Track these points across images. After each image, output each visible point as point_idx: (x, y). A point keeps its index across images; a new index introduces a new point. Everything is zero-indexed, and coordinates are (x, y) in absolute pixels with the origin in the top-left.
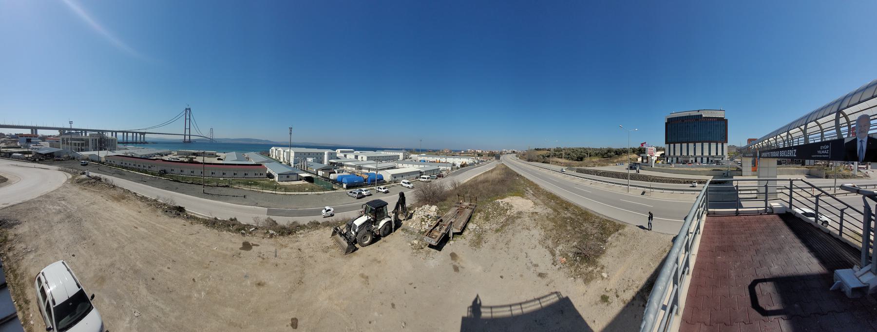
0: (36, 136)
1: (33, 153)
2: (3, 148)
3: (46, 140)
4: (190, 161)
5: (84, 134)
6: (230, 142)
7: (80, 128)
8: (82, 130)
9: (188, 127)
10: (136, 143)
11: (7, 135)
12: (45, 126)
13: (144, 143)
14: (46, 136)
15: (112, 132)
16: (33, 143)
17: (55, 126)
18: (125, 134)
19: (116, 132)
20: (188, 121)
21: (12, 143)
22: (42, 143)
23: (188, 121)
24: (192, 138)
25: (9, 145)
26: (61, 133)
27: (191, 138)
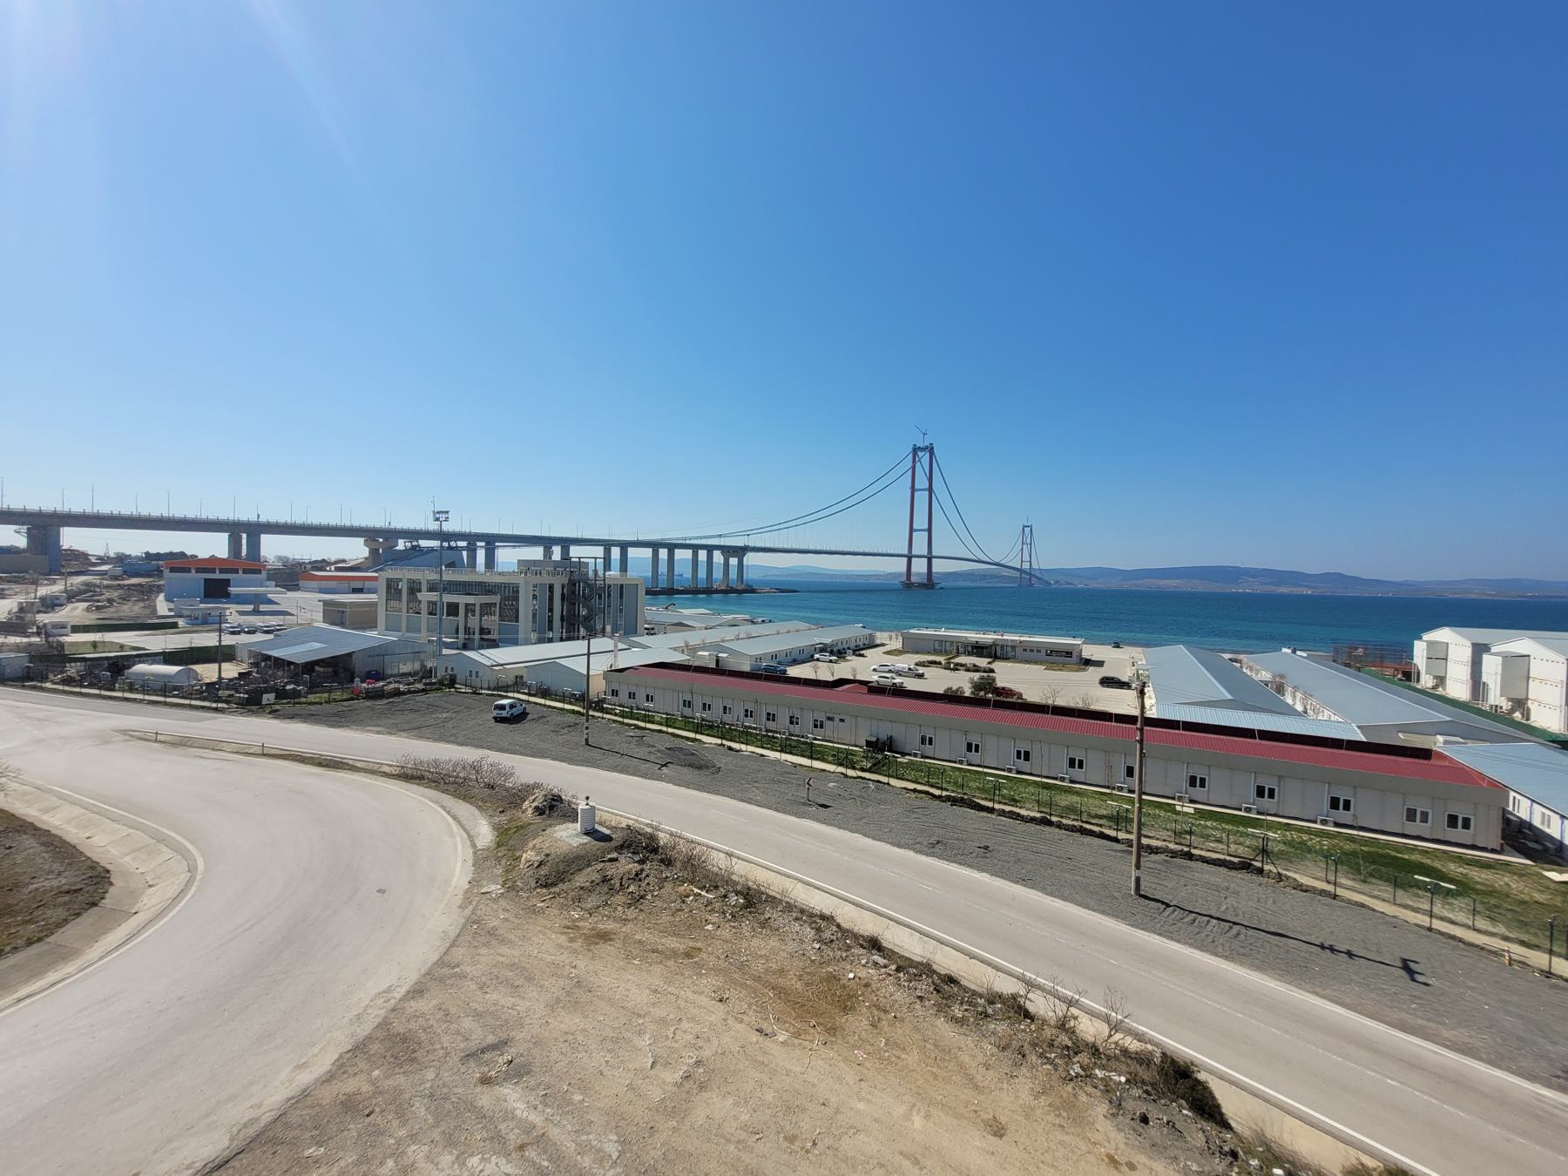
0: (254, 565)
1: (242, 654)
2: (76, 629)
3: (302, 583)
4: (977, 687)
5: (481, 555)
7: (466, 529)
8: (472, 538)
9: (921, 522)
10: (709, 591)
11: (103, 560)
12: (299, 519)
13: (739, 591)
14: (301, 564)
15: (607, 545)
16: (240, 599)
17: (346, 522)
18: (663, 553)
19: (624, 546)
20: (921, 498)
21: (124, 599)
22: (287, 599)
23: (921, 498)
24: (939, 567)
25: (110, 612)
26: (374, 552)
27: (934, 570)
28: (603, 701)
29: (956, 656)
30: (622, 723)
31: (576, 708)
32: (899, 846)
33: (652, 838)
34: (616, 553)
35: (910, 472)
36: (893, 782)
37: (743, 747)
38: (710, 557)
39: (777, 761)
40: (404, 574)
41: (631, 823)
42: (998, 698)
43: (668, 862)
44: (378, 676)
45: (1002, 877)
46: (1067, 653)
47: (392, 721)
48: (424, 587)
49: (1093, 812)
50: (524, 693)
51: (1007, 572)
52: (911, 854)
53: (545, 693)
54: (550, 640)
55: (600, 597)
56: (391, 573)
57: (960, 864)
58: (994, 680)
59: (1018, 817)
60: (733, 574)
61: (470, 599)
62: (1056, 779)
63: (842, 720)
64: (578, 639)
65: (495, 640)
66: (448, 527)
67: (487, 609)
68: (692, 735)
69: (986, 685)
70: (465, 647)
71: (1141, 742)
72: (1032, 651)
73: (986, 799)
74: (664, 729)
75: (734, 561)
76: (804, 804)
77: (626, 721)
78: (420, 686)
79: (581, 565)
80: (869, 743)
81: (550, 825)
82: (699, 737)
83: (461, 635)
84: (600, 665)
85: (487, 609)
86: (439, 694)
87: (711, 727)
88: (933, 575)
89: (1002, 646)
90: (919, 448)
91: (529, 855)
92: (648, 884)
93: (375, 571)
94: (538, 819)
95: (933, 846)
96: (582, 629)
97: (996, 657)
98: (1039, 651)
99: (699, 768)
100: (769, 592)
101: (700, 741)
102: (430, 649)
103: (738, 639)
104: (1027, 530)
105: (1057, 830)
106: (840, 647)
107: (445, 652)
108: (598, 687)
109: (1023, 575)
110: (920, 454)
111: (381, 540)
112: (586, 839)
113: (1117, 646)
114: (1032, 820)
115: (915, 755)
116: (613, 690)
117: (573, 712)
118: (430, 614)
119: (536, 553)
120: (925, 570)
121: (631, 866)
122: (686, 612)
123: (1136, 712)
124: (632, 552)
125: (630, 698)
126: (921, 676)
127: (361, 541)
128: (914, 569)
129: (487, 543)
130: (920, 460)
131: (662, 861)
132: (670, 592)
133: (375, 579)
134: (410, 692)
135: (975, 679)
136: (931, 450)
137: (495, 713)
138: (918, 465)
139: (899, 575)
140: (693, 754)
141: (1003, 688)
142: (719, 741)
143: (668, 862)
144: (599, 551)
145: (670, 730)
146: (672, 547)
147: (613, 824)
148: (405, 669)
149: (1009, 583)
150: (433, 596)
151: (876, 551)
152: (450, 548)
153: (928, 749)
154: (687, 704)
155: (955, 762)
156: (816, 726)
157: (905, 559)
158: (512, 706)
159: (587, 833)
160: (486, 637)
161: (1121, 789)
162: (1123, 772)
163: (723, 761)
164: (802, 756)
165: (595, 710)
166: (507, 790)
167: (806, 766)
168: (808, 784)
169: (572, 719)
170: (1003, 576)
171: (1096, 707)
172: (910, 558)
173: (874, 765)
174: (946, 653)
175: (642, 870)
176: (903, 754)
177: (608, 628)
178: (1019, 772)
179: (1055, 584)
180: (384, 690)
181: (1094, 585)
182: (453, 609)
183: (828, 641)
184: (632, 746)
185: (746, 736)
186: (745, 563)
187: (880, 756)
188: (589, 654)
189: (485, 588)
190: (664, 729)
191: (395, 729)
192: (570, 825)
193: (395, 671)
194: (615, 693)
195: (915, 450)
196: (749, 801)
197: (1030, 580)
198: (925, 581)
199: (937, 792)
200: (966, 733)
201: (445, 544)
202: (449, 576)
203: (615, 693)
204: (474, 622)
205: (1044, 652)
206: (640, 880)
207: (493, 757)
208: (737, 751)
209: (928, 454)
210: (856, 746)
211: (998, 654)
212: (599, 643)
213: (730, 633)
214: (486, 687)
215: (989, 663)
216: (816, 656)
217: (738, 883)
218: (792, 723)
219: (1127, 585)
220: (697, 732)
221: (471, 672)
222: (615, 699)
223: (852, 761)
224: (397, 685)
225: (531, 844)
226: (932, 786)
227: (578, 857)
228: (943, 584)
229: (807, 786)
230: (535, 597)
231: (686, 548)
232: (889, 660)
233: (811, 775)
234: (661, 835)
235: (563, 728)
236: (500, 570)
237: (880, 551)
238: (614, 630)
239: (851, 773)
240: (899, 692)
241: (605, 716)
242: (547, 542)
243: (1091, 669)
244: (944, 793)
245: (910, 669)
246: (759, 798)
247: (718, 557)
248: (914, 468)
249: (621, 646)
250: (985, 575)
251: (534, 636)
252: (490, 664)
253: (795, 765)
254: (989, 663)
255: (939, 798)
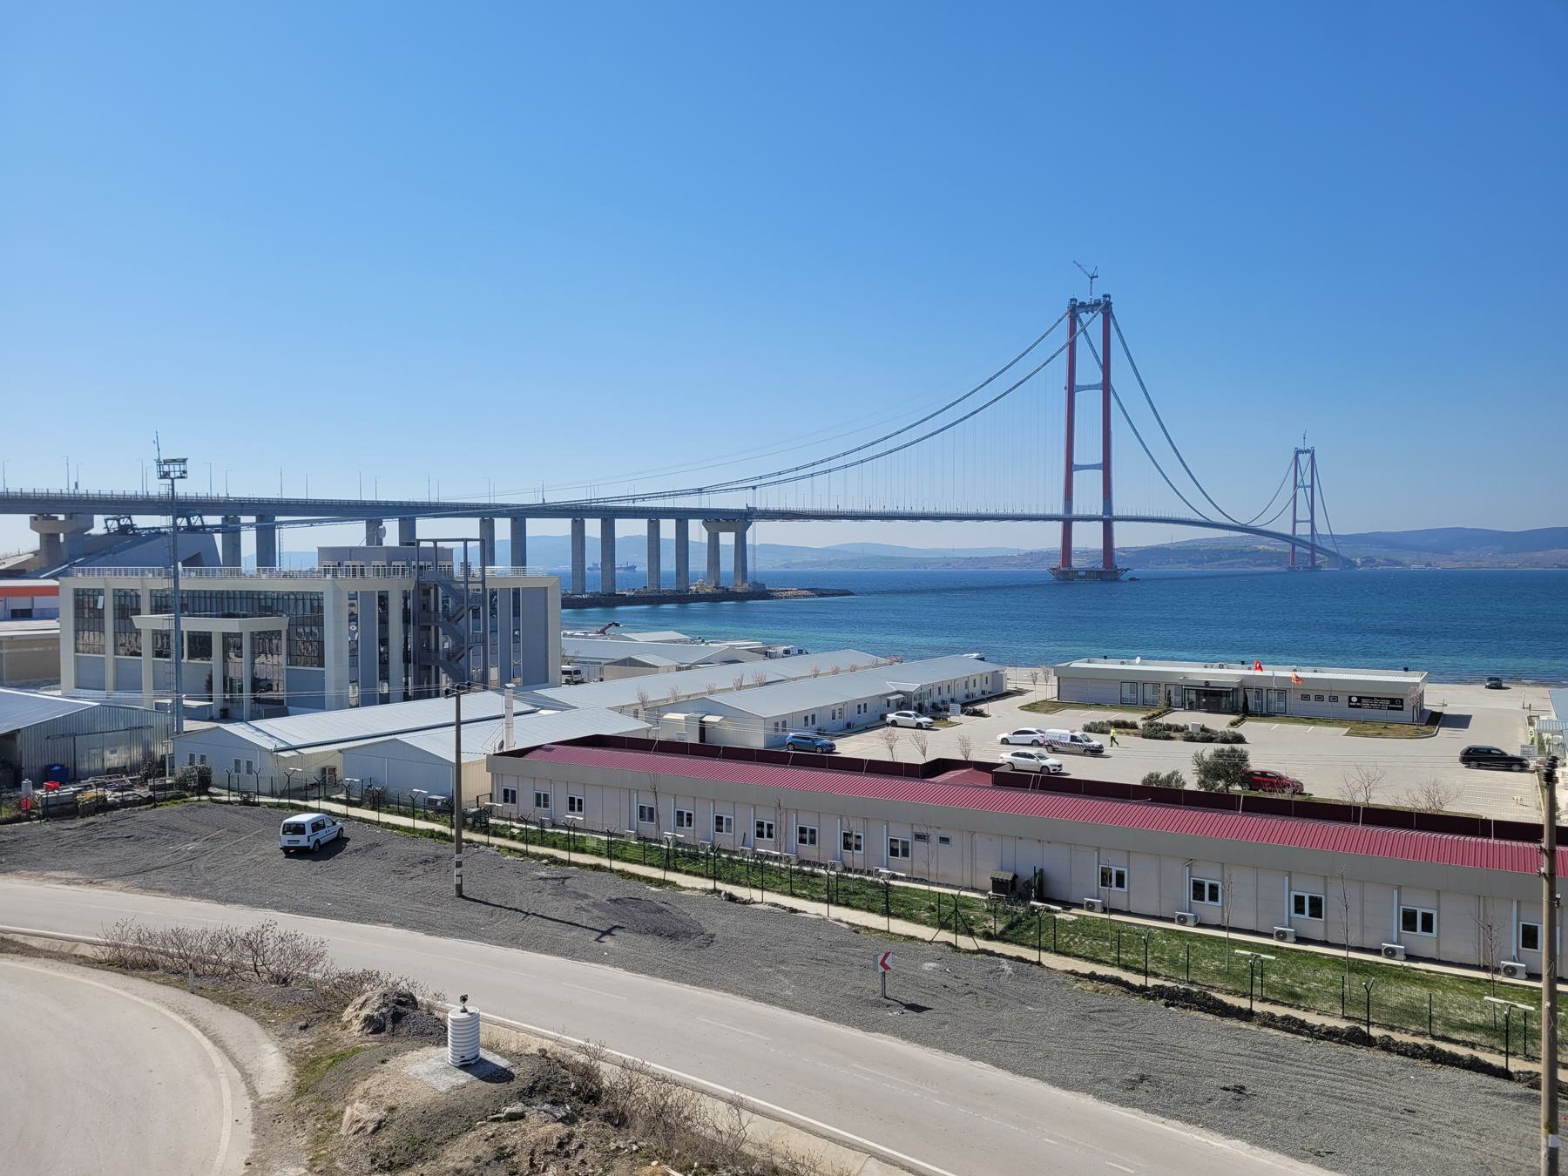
4: (1210, 771)
5: (249, 541)
6: (1487, 561)
7: (219, 491)
9: (1088, 449)
10: (682, 597)
15: (487, 514)
18: (593, 527)
19: (519, 515)
20: (1090, 403)
24: (1127, 537)
26: (49, 540)
28: (488, 812)
29: (1166, 712)
30: (525, 854)
31: (437, 827)
32: (1066, 1085)
33: (588, 1073)
34: (503, 528)
35: (1066, 351)
36: (1050, 960)
37: (756, 895)
38: (682, 532)
39: (822, 922)
40: (107, 580)
41: (547, 1044)
42: (1253, 793)
43: (619, 1120)
44: (62, 774)
45: (1274, 1148)
46: (1393, 701)
47: (96, 859)
48: (145, 604)
49: (1456, 1019)
50: (339, 801)
51: (1263, 545)
52: (1087, 1102)
53: (378, 801)
54: (385, 700)
55: (476, 612)
56: (84, 579)
57: (1189, 1121)
58: (1244, 758)
59: (1300, 1027)
60: (727, 564)
61: (232, 625)
62: (1378, 952)
63: (944, 840)
64: (437, 695)
65: (280, 702)
66: (184, 489)
67: (263, 643)
68: (657, 873)
69: (1230, 767)
70: (226, 716)
71: (1551, 877)
72: (1319, 698)
73: (1235, 993)
74: (605, 862)
75: (727, 539)
76: (877, 1004)
77: (533, 849)
78: (144, 792)
79: (438, 554)
80: (998, 885)
81: (396, 1052)
82: (671, 876)
83: (217, 694)
84: (480, 744)
85: (263, 643)
86: (178, 806)
87: (694, 857)
88: (1117, 554)
89: (1259, 691)
90: (1083, 305)
91: (358, 1110)
92: (583, 1162)
93: (54, 577)
94: (372, 1041)
95: (1133, 1085)
96: (443, 677)
97: (1245, 712)
98: (1334, 699)
99: (673, 936)
100: (796, 596)
101: (673, 884)
102: (160, 720)
103: (740, 687)
104: (1304, 459)
105: (1382, 1055)
106: (937, 698)
107: (189, 725)
108: (477, 785)
109: (1298, 549)
110: (1085, 317)
111: (61, 517)
112: (463, 1078)
113: (1496, 684)
114: (1331, 1034)
115: (1091, 907)
116: (506, 791)
117: (432, 834)
118: (159, 654)
119: (352, 534)
120: (1098, 544)
121: (549, 1127)
122: (641, 638)
123: (1538, 817)
124: (534, 527)
125: (538, 804)
126: (1097, 752)
127: (24, 519)
128: (1076, 544)
129: (260, 518)
130: (1084, 330)
131: (608, 1117)
132: (609, 600)
133: (53, 591)
134: (124, 804)
135: (1206, 757)
136: (1105, 308)
137: (286, 839)
138: (1080, 339)
139: (1047, 555)
140: (661, 911)
141: (1264, 774)
142: (710, 884)
143: (619, 1120)
144: (470, 527)
145: (617, 865)
146: (608, 516)
147: (513, 1047)
148: (114, 759)
149: (1269, 565)
150: (163, 621)
151: (1001, 512)
152: (191, 529)
153: (1116, 895)
154: (648, 814)
155: (1171, 920)
156: (894, 852)
157: (1060, 524)
158: (316, 826)
159: (465, 1066)
160: (264, 695)
161: (1511, 972)
162: (1514, 938)
163: (720, 922)
164: (870, 910)
165: (472, 829)
166: (313, 985)
167: (880, 931)
168: (883, 964)
169: (428, 848)
170: (1258, 551)
171: (1454, 808)
172: (1068, 522)
173: (1011, 927)
174: (1145, 705)
175: (571, 1136)
176: (1067, 905)
177: (494, 674)
178: (1300, 940)
179: (1363, 563)
180: (76, 803)
181: (1444, 564)
182: (200, 645)
183: (912, 687)
184: (545, 897)
185: (760, 874)
186: (749, 541)
187: (1021, 910)
188: (458, 724)
189: (260, 604)
190: (605, 862)
191: (99, 875)
192: (432, 1051)
193: (97, 765)
194: (509, 796)
195: (1075, 309)
196: (771, 999)
197: (1313, 558)
198: (1100, 566)
199: (1137, 980)
200: (1190, 863)
201: (182, 522)
202: (191, 581)
203: (509, 796)
204: (240, 668)
205: (1343, 700)
206: (567, 1155)
207: (286, 923)
208: (745, 903)
209: (1100, 315)
210: (974, 890)
211: (1251, 706)
212: (476, 703)
213: (722, 677)
214: (268, 790)
215: (1233, 724)
216: (891, 717)
217: (753, 1160)
218: (847, 846)
219: (1514, 562)
220: (667, 868)
221: (237, 762)
222: (510, 808)
223: (966, 920)
224: (100, 792)
225: (359, 1090)
226: (1126, 968)
227: (450, 1113)
228: (1137, 571)
229: (881, 969)
230: (353, 618)
231: (635, 517)
232: (1032, 721)
233: (889, 946)
234: (604, 1067)
235: (414, 865)
236: (286, 568)
237: (1010, 512)
238: (506, 677)
239: (965, 942)
240: (1054, 783)
241: (493, 840)
242: (372, 513)
243: (1444, 732)
244: (1152, 982)
245: (1073, 738)
246: (788, 993)
247: (697, 531)
248: (1072, 346)
249: (519, 706)
250: (1221, 551)
251: (353, 692)
252: (271, 747)
253: (856, 929)
254: (1233, 724)
255: (1142, 990)
